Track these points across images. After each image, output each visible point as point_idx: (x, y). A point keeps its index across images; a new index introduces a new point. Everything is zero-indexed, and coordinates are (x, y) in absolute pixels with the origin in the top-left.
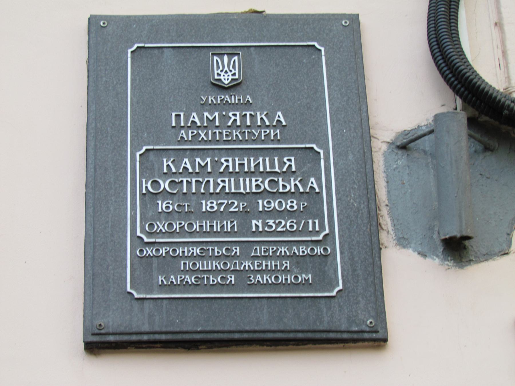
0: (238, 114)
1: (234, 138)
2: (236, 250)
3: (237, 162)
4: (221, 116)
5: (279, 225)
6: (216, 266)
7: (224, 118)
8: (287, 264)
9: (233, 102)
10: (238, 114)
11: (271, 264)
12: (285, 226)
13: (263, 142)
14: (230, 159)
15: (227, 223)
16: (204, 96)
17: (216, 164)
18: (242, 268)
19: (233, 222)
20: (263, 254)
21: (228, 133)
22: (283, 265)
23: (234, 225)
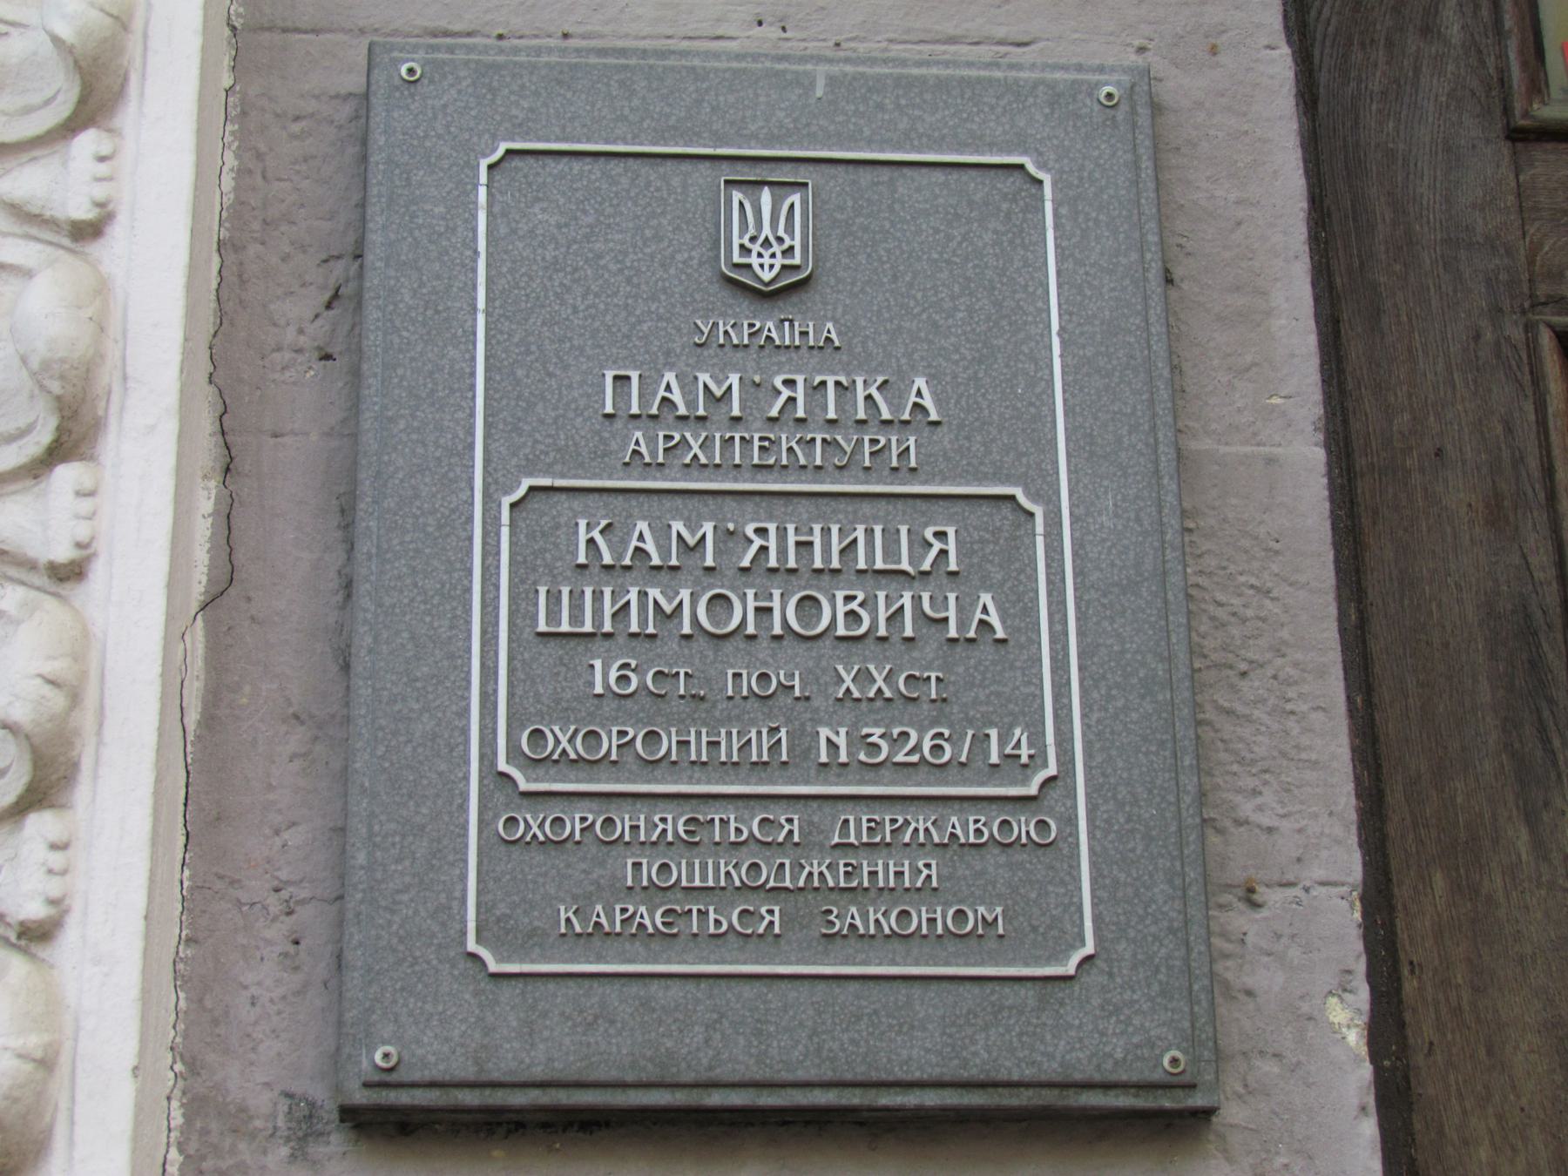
0: (800, 379)
2: (791, 824)
3: (792, 539)
5: (899, 743)
6: (728, 873)
8: (932, 869)
10: (800, 379)
11: (885, 869)
12: (917, 748)
14: (772, 527)
15: (759, 733)
16: (706, 318)
18: (801, 884)
20: (865, 839)
21: (766, 444)
22: (921, 872)
23: (780, 739)
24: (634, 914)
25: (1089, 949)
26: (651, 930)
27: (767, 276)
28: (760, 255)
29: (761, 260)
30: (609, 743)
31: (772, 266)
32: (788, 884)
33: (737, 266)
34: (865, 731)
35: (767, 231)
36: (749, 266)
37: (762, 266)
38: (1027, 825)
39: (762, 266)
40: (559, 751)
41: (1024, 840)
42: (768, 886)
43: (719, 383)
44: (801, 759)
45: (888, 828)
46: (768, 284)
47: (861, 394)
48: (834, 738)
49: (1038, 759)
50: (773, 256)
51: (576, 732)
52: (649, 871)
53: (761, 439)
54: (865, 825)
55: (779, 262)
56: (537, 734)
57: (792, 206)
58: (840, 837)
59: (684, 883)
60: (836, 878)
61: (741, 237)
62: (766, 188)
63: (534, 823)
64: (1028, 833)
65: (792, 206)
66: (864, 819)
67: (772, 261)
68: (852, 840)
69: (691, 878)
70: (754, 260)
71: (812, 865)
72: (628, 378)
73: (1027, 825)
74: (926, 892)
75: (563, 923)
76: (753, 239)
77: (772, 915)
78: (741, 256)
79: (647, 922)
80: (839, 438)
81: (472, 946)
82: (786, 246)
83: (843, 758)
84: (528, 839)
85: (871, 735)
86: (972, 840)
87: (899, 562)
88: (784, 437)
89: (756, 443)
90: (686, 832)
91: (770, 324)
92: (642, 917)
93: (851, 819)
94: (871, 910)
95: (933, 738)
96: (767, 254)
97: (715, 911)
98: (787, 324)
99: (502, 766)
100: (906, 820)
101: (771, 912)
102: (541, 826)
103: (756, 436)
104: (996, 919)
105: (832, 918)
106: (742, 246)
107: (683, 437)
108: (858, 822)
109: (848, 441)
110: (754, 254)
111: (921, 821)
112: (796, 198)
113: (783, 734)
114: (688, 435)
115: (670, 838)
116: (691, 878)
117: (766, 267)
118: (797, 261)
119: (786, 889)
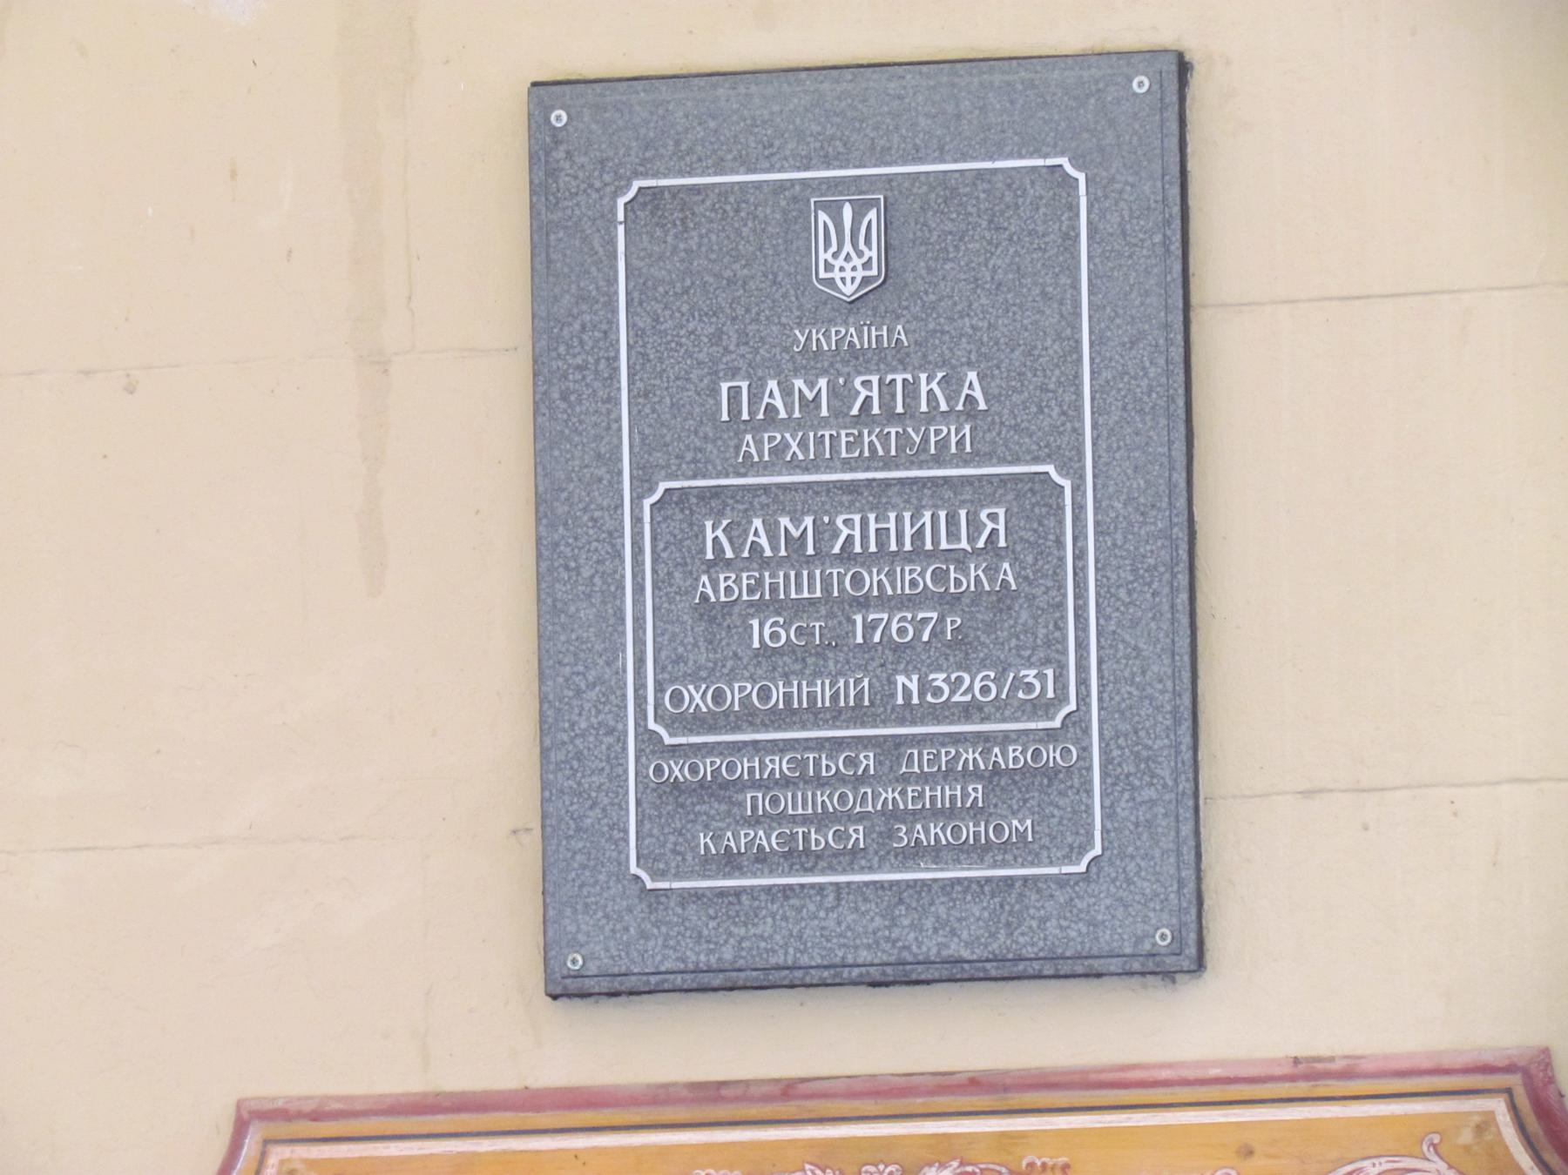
0: (875, 379)
1: (866, 454)
4: (833, 390)
7: (842, 395)
9: (866, 346)
13: (938, 461)
17: (825, 532)
19: (861, 680)
21: (851, 439)
24: (756, 835)
25: (1097, 851)
26: (768, 850)
27: (849, 289)
28: (842, 269)
29: (843, 275)
30: (733, 697)
31: (853, 279)
32: (870, 809)
33: (819, 280)
34: (931, 677)
35: (848, 247)
36: (830, 282)
37: (843, 279)
38: (1054, 751)
39: (843, 279)
40: (694, 705)
41: (1051, 765)
42: (855, 812)
43: (811, 388)
44: (881, 706)
45: (944, 759)
46: (849, 297)
47: (924, 389)
48: (907, 683)
49: (1061, 698)
50: (854, 269)
51: (707, 688)
52: (764, 804)
53: (847, 435)
54: (926, 757)
55: (860, 274)
56: (677, 698)
57: (870, 222)
58: (906, 767)
59: (790, 812)
60: (905, 803)
61: (826, 251)
62: (847, 204)
63: (677, 770)
64: (1054, 758)
65: (870, 222)
66: (925, 752)
67: (854, 274)
68: (916, 769)
69: (794, 807)
70: (837, 275)
71: (887, 792)
72: (740, 387)
73: (1054, 751)
74: (976, 812)
75: (702, 847)
76: (835, 255)
77: (857, 833)
78: (826, 270)
79: (765, 843)
80: (910, 430)
81: (634, 869)
82: (865, 259)
83: (915, 700)
84: (672, 780)
85: (934, 680)
86: (1011, 766)
87: (959, 540)
88: (866, 432)
89: (844, 440)
90: (788, 768)
91: (852, 330)
92: (760, 839)
93: (916, 752)
94: (932, 825)
95: (982, 680)
96: (848, 266)
97: (816, 833)
98: (866, 328)
99: (652, 725)
100: (957, 752)
101: (856, 831)
102: (681, 770)
103: (843, 433)
104: (1027, 828)
105: (901, 834)
106: (826, 261)
107: (783, 437)
108: (920, 754)
109: (917, 431)
110: (837, 269)
111: (970, 755)
112: (872, 215)
113: (866, 683)
114: (787, 435)
115: (777, 776)
116: (794, 807)
117: (848, 281)
118: (874, 272)
119: (869, 812)
